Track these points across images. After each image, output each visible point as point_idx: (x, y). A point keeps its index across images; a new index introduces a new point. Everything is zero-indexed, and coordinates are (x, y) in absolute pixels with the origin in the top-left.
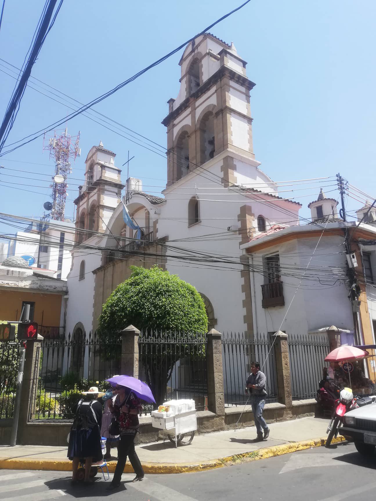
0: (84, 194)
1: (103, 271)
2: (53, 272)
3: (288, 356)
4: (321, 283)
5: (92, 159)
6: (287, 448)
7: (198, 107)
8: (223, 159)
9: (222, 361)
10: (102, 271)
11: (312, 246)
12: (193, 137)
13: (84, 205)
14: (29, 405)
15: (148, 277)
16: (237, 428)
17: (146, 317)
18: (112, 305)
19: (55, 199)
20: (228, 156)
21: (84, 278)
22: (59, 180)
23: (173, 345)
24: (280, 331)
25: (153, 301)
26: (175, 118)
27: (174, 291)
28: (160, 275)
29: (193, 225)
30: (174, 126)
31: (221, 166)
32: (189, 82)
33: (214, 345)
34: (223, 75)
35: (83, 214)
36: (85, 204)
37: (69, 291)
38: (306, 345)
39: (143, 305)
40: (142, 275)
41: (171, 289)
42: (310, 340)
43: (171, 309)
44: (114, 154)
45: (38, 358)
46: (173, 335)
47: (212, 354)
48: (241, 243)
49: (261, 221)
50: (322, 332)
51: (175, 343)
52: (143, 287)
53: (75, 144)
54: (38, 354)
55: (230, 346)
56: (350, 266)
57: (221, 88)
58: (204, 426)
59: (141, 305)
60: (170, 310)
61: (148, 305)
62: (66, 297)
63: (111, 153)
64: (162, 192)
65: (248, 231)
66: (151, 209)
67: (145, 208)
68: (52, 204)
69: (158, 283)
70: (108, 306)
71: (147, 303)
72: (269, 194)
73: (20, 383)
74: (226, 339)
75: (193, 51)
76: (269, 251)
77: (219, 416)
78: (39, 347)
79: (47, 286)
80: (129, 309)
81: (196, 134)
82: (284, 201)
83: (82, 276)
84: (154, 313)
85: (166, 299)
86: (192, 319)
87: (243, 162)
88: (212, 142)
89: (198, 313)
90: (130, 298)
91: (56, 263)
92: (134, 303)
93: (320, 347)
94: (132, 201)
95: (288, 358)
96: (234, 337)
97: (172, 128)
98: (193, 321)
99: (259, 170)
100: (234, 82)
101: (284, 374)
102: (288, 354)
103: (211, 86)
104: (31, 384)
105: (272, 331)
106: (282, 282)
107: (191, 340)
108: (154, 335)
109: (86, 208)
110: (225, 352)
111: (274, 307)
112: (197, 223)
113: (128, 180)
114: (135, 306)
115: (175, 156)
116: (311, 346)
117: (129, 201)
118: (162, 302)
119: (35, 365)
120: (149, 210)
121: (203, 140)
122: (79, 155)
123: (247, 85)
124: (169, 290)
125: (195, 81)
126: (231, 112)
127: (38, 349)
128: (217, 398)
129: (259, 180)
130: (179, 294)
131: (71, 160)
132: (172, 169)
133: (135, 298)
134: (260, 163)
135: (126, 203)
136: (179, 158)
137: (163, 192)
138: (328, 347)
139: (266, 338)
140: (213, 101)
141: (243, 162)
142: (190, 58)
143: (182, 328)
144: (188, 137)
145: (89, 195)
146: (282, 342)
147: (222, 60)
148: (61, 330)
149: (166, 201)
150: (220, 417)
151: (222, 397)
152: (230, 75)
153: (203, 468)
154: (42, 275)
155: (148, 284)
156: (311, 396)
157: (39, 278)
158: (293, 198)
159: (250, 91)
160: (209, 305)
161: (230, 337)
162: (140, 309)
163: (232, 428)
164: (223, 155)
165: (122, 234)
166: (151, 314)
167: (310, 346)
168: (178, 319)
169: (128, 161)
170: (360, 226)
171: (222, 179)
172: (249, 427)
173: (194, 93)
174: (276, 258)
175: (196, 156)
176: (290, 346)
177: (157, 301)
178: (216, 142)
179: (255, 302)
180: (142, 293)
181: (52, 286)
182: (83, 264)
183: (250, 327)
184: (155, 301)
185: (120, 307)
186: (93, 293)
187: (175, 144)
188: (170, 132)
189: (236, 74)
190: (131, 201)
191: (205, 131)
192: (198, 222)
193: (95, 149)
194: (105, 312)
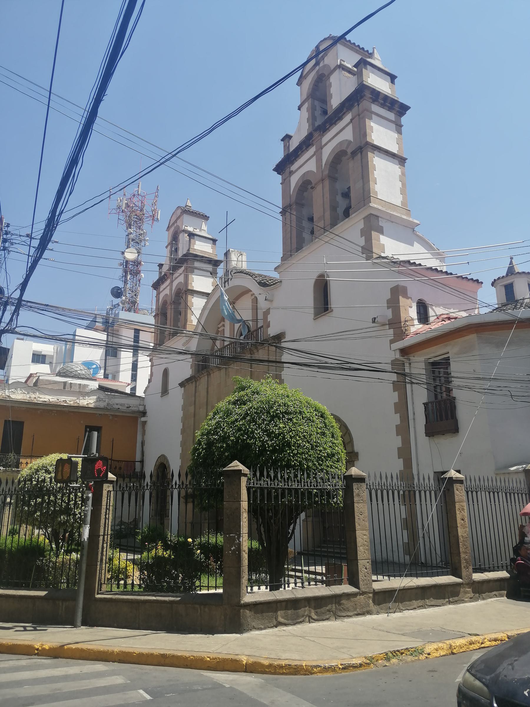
0: (165, 275)
1: (194, 383)
2: (125, 384)
3: (465, 508)
4: (513, 399)
5: (175, 225)
6: (467, 644)
7: (326, 144)
8: (364, 218)
9: (367, 514)
10: (192, 383)
11: (500, 345)
12: (319, 188)
13: (166, 290)
14: (98, 571)
15: (258, 393)
16: (391, 611)
17: (257, 449)
18: (209, 433)
19: (126, 282)
20: (371, 214)
21: (168, 394)
22: (131, 255)
23: (296, 490)
24: (452, 470)
25: (266, 427)
26: (292, 163)
27: (296, 413)
28: (276, 389)
29: (320, 316)
30: (291, 173)
31: (361, 229)
32: (312, 110)
33: (356, 491)
34: (362, 97)
35: (165, 303)
36: (169, 288)
38: (493, 491)
39: (253, 432)
40: (249, 390)
41: (291, 411)
42: (499, 484)
43: (292, 439)
44: (206, 216)
45: (109, 506)
46: (296, 476)
47: (353, 503)
48: (392, 342)
49: (421, 308)
50: (516, 472)
51: (299, 487)
52: (251, 408)
53: (152, 205)
54: (108, 501)
55: (379, 492)
57: (359, 116)
58: (342, 608)
59: (249, 433)
60: (290, 440)
61: (259, 432)
62: (143, 419)
63: (202, 215)
64: (276, 269)
65: (402, 324)
66: (260, 294)
67: (251, 293)
68: (123, 289)
69: (273, 401)
70: (203, 435)
71: (257, 431)
72: (433, 268)
73: (86, 540)
74: (373, 483)
75: (317, 64)
77: (363, 593)
78: (110, 491)
79: (117, 404)
80: (232, 438)
81: (323, 184)
82: (456, 279)
83: (165, 391)
84: (268, 444)
85: (285, 424)
86: (323, 453)
87: (392, 222)
88: (346, 195)
89: (331, 444)
90: (233, 423)
91: (130, 373)
92: (240, 429)
93: (514, 494)
94: (232, 283)
95: (466, 511)
96: (384, 480)
97: (287, 177)
98: (325, 457)
99: (418, 233)
101: (460, 534)
102: (465, 504)
103: (344, 113)
104: (101, 542)
105: (441, 470)
106: (454, 398)
107: (322, 484)
108: (268, 476)
109: (169, 294)
110: (371, 501)
111: (444, 435)
112: (326, 312)
113: (227, 254)
114: (241, 435)
115: (294, 217)
116: (500, 494)
117: (228, 284)
118: (278, 429)
119: (106, 515)
120: (256, 296)
121: (333, 192)
122: (158, 219)
123: (398, 109)
124: (288, 411)
125: (321, 107)
126: (375, 150)
127: (109, 494)
128: (360, 566)
129: (418, 247)
130: (303, 417)
131: (146, 227)
132: (289, 235)
133: (240, 423)
134: (418, 222)
136: (299, 220)
137: (276, 269)
138: (526, 494)
139: (432, 481)
140: (348, 135)
141: (392, 222)
142: (313, 74)
143: (308, 466)
144: (312, 188)
145: (173, 276)
146: (456, 486)
147: (359, 74)
148: (138, 465)
149: (281, 282)
150: (365, 595)
151: (369, 566)
152: (371, 96)
153: (343, 668)
154: (111, 389)
155: (258, 403)
156: (500, 568)
157: (106, 393)
158: (470, 274)
159: (402, 118)
160: (346, 432)
161: (378, 479)
162: (247, 438)
163: (383, 611)
164: (364, 213)
165: (220, 330)
166: (263, 445)
167: (498, 493)
168: (303, 453)
169: (226, 227)
171: (362, 247)
172: (409, 610)
173: (319, 126)
174: (446, 363)
175: (324, 216)
176: (467, 492)
177: (272, 428)
178: (352, 195)
179: (415, 428)
180: (251, 416)
181: (124, 404)
182: (166, 373)
183: (408, 463)
184: (269, 427)
185: (220, 436)
186: (180, 414)
187: (293, 199)
188: (285, 183)
189: (380, 94)
190: (232, 283)
191: (337, 179)
192: (328, 312)
193: (179, 211)
194: (199, 443)
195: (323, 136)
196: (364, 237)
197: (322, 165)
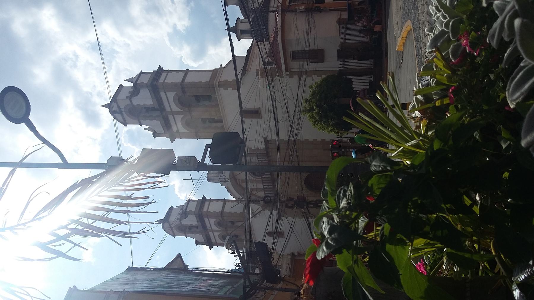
5: (173, 229)
13: (215, 236)
30: (178, 131)
32: (145, 118)
37: (291, 252)
38: (346, 35)
56: (304, 10)
62: (296, 254)
75: (121, 113)
76: (289, 56)
79: (286, 271)
100: (159, 79)
126: (184, 81)
135: (228, 182)
140: (171, 95)
142: (125, 115)
145: (207, 229)
152: (156, 82)
170: (281, 3)
193: (166, 225)
195: (166, 110)
196: (228, 89)
197: (181, 111)
